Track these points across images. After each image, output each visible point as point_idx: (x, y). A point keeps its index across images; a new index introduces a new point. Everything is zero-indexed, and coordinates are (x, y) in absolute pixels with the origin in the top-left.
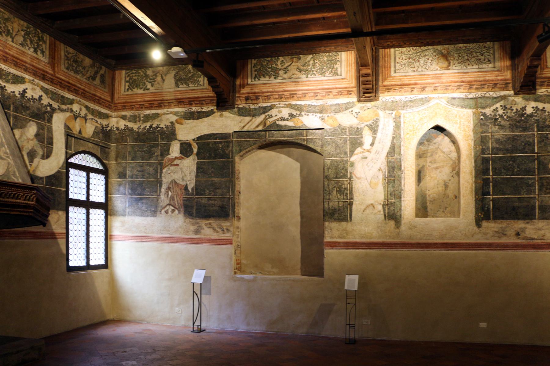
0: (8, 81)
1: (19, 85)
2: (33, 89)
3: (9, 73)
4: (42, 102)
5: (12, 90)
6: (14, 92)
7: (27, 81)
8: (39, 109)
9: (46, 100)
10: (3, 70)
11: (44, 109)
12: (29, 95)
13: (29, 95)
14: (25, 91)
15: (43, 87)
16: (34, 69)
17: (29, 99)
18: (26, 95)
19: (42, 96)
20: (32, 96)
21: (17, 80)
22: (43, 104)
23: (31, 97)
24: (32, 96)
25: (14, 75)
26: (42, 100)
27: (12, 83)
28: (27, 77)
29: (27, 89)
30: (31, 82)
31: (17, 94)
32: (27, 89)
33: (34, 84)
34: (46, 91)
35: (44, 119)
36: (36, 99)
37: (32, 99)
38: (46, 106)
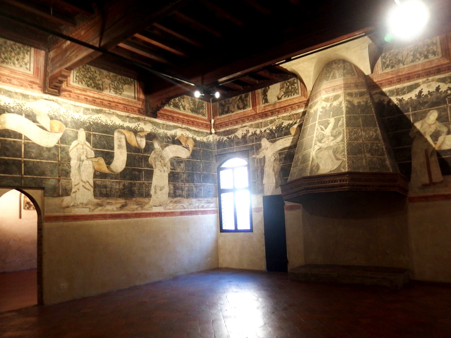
0: (404, 94)
1: (415, 90)
2: (428, 86)
3: (404, 88)
4: (440, 90)
5: (409, 97)
6: (411, 98)
7: (421, 83)
8: (438, 98)
9: (444, 87)
10: (399, 89)
11: (443, 95)
12: (425, 92)
13: (425, 92)
14: (421, 92)
15: (439, 79)
16: (427, 71)
17: (426, 96)
18: (423, 94)
19: (439, 86)
20: (429, 92)
21: (411, 89)
22: (442, 91)
23: (427, 93)
24: (429, 92)
25: (408, 87)
26: (440, 89)
27: (408, 93)
28: (420, 81)
29: (422, 89)
30: (424, 82)
31: (414, 98)
32: (422, 89)
33: (429, 82)
34: (443, 80)
35: (445, 102)
36: (434, 92)
37: (428, 94)
38: (446, 91)
